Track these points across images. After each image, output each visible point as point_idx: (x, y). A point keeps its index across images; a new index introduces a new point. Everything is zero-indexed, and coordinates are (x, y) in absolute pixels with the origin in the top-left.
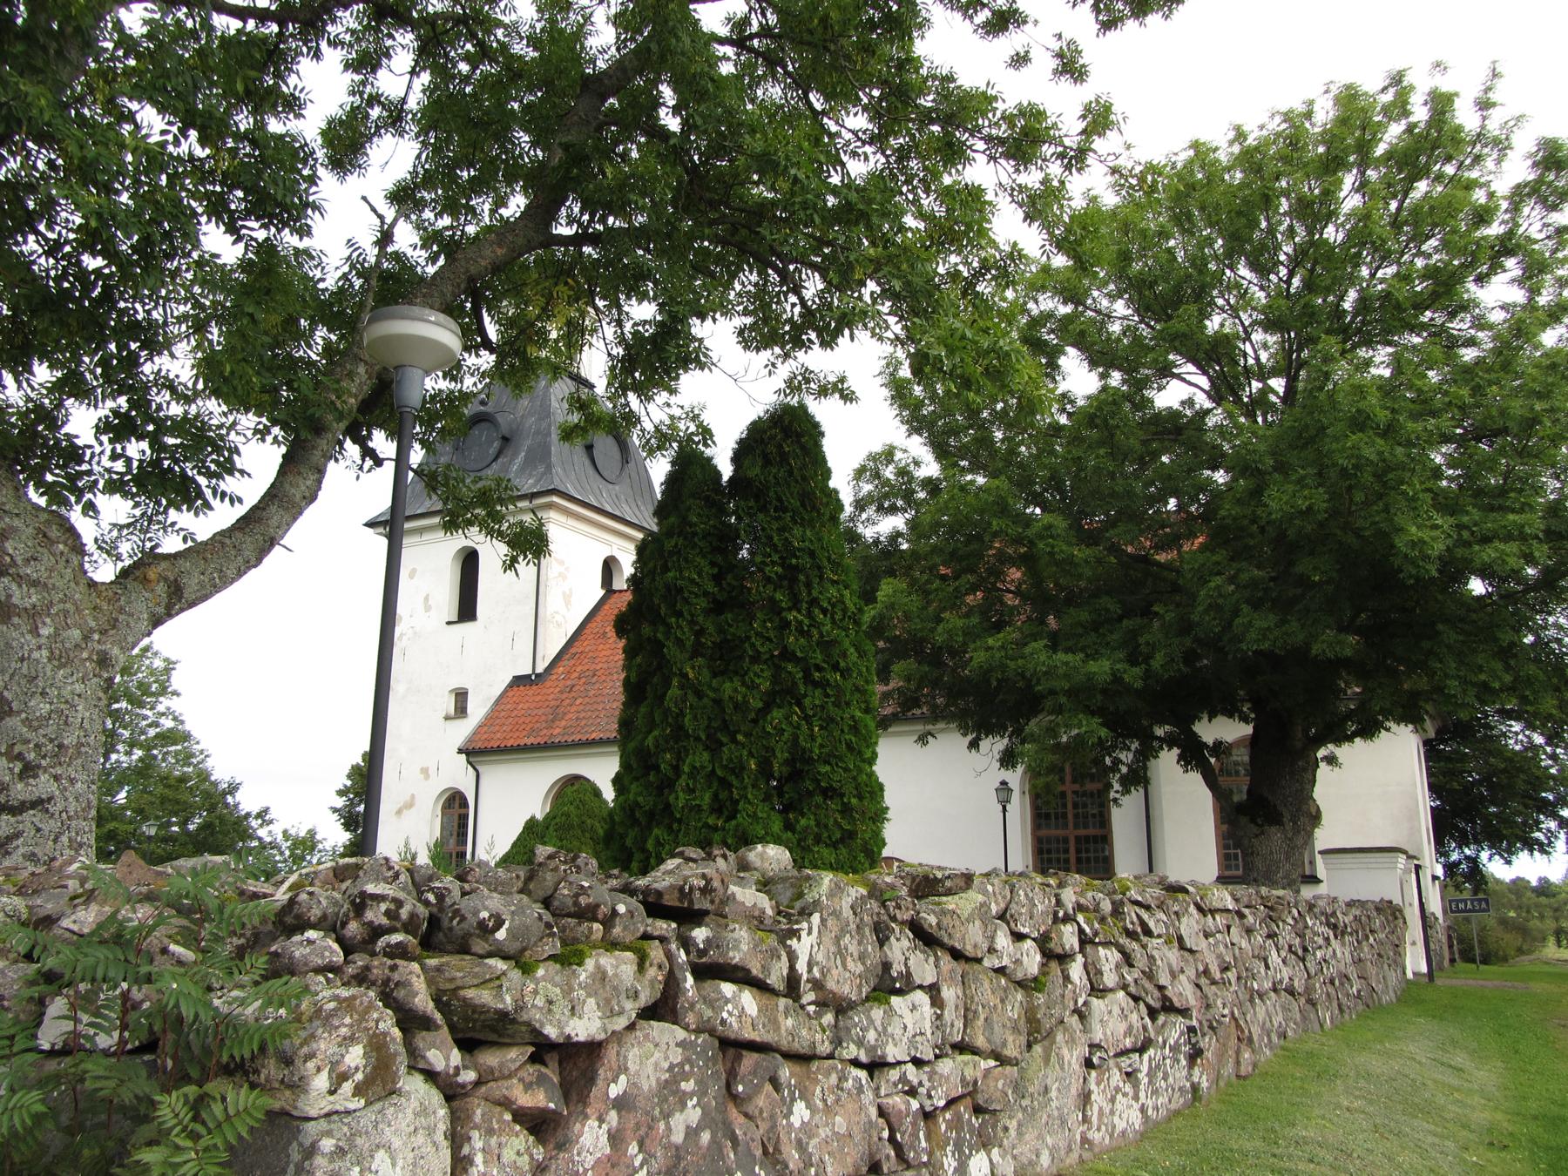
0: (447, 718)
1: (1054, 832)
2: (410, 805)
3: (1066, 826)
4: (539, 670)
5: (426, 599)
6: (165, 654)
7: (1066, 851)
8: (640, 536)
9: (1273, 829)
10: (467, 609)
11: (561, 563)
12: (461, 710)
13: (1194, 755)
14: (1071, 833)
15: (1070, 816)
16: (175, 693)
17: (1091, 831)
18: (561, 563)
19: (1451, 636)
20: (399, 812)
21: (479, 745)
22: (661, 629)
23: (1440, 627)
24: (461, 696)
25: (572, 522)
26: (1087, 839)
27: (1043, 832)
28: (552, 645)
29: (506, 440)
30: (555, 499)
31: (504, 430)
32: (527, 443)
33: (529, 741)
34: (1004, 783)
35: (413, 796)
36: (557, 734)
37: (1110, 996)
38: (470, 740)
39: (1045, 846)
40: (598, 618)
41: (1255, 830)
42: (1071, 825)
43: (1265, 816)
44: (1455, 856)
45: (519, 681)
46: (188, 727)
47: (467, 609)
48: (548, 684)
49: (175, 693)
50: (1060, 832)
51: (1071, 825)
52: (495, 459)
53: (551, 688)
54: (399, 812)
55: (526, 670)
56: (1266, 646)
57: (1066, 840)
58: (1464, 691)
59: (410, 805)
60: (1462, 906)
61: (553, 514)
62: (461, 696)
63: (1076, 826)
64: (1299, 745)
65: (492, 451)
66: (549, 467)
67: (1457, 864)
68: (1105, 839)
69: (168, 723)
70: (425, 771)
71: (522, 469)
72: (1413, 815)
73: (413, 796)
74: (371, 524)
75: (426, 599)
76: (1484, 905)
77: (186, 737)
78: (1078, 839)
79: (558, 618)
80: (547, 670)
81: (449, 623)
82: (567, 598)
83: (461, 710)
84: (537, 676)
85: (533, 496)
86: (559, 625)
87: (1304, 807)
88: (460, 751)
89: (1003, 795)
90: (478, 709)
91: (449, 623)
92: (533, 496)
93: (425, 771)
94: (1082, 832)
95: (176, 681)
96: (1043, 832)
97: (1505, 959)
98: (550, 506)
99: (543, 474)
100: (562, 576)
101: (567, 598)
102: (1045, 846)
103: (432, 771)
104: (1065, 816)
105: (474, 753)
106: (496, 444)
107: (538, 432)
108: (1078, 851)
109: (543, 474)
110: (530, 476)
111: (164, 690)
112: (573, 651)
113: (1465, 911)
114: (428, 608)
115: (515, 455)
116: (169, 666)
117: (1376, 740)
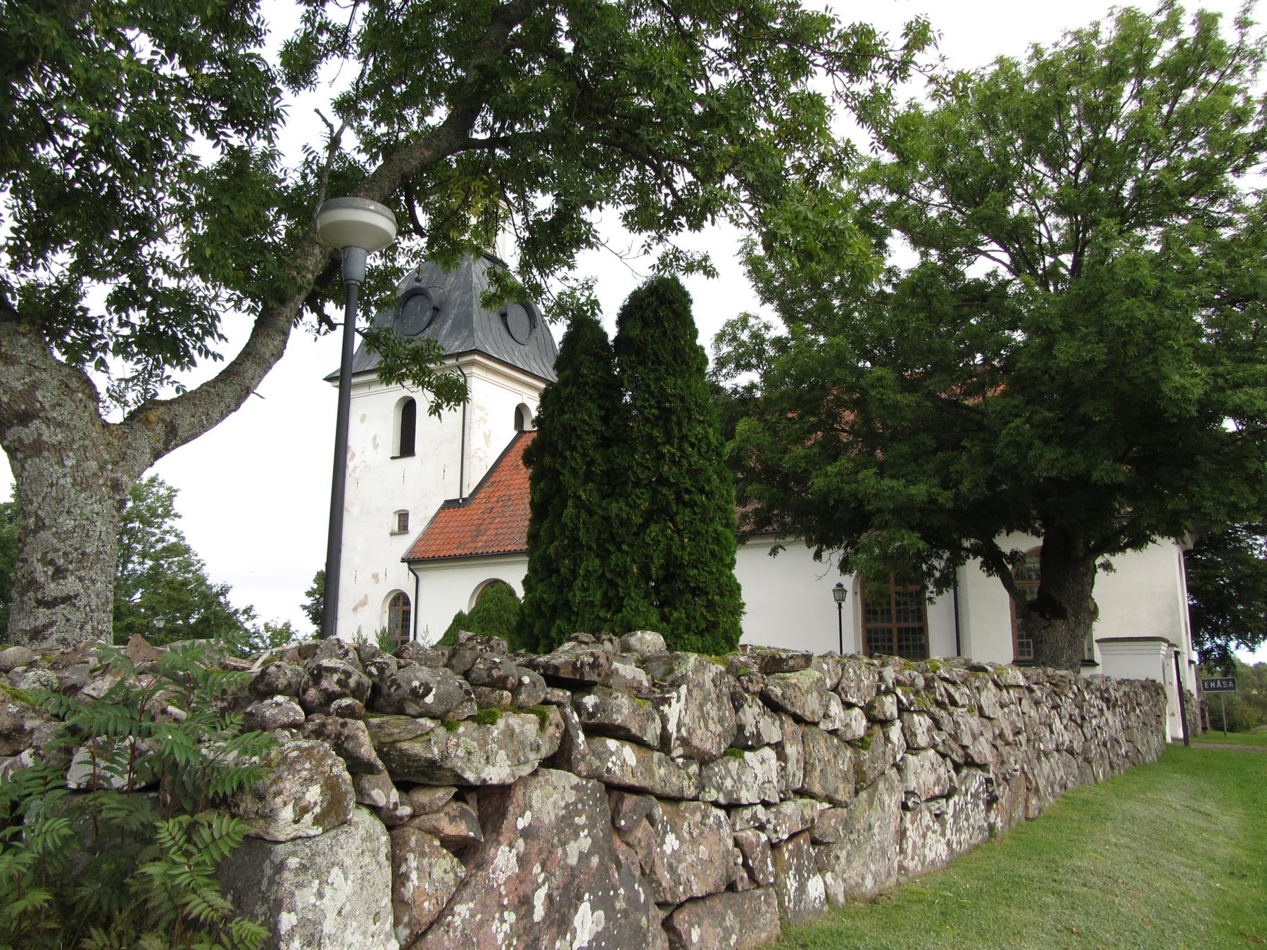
0: (392, 534)
1: (880, 625)
2: (364, 603)
3: (890, 620)
4: (466, 495)
5: (375, 438)
6: (168, 484)
7: (890, 640)
8: (543, 386)
9: (1059, 622)
10: (407, 447)
12: (403, 527)
13: (994, 562)
14: (894, 625)
15: (893, 612)
16: (176, 515)
17: (910, 624)
18: (482, 409)
19: (1207, 465)
20: (355, 609)
21: (418, 555)
22: (559, 460)
23: (1199, 458)
24: (403, 517)
25: (490, 376)
26: (907, 630)
27: (872, 625)
28: (475, 475)
29: (436, 310)
30: (477, 357)
31: (435, 302)
32: (453, 312)
33: (457, 552)
34: (840, 585)
35: (366, 596)
36: (480, 546)
37: (923, 753)
38: (411, 551)
39: (873, 636)
40: (512, 453)
41: (1044, 623)
42: (894, 620)
43: (1052, 614)
44: (1208, 645)
45: (449, 504)
46: (187, 542)
47: (407, 447)
48: (473, 506)
49: (176, 515)
50: (885, 625)
51: (894, 620)
52: (428, 325)
53: (475, 511)
54: (355, 609)
56: (1054, 473)
57: (890, 631)
58: (1217, 510)
59: (364, 603)
60: (1213, 685)
61: (475, 370)
62: (403, 517)
63: (898, 620)
64: (1081, 554)
65: (426, 319)
66: (471, 332)
67: (1210, 651)
68: (922, 630)
69: (172, 539)
70: (375, 576)
71: (450, 333)
72: (1175, 611)
73: (366, 596)
76: (1231, 684)
77: (187, 550)
78: (899, 630)
79: (480, 454)
80: (471, 495)
81: (392, 458)
82: (487, 437)
83: (403, 527)
85: (459, 355)
86: (481, 459)
87: (1084, 605)
88: (403, 560)
89: (839, 595)
90: (417, 527)
91: (392, 458)
92: (459, 355)
93: (375, 576)
94: (903, 625)
95: (178, 505)
96: (872, 625)
97: (1247, 728)
98: (473, 363)
99: (468, 337)
100: (483, 419)
101: (487, 437)
102: (873, 636)
103: (381, 576)
104: (889, 612)
105: (414, 561)
106: (428, 313)
107: (462, 304)
108: (900, 640)
109: (468, 337)
110: (457, 339)
111: (167, 513)
112: (492, 480)
113: (1216, 689)
114: (376, 446)
115: (444, 322)
116: (172, 493)
117: (1144, 551)
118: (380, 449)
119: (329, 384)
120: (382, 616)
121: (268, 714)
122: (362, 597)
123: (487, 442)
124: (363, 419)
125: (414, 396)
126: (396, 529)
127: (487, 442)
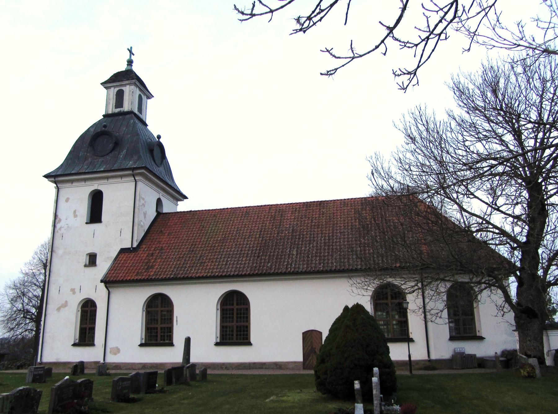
0: (85, 266)
2: (65, 305)
4: (135, 245)
5: (75, 212)
11: (143, 199)
20: (59, 309)
35: (66, 302)
45: (123, 251)
52: (111, 152)
53: (143, 254)
55: (129, 246)
59: (65, 305)
70: (73, 291)
71: (125, 157)
73: (66, 302)
74: (47, 176)
75: (75, 212)
82: (145, 214)
84: (134, 248)
88: (102, 281)
92: (133, 169)
93: (73, 291)
103: (77, 290)
106: (111, 146)
110: (130, 160)
112: (148, 238)
114: (75, 216)
118: (78, 218)
119: (46, 179)
120: (77, 314)
121: (398, 373)
122: (64, 302)
123: (145, 217)
124: (67, 200)
125: (101, 188)
126: (88, 263)
127: (145, 217)
